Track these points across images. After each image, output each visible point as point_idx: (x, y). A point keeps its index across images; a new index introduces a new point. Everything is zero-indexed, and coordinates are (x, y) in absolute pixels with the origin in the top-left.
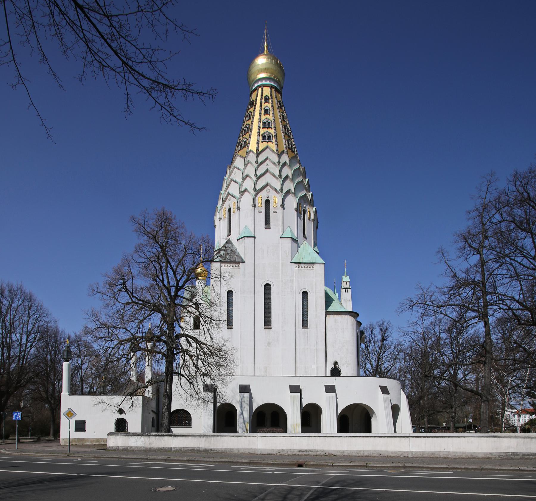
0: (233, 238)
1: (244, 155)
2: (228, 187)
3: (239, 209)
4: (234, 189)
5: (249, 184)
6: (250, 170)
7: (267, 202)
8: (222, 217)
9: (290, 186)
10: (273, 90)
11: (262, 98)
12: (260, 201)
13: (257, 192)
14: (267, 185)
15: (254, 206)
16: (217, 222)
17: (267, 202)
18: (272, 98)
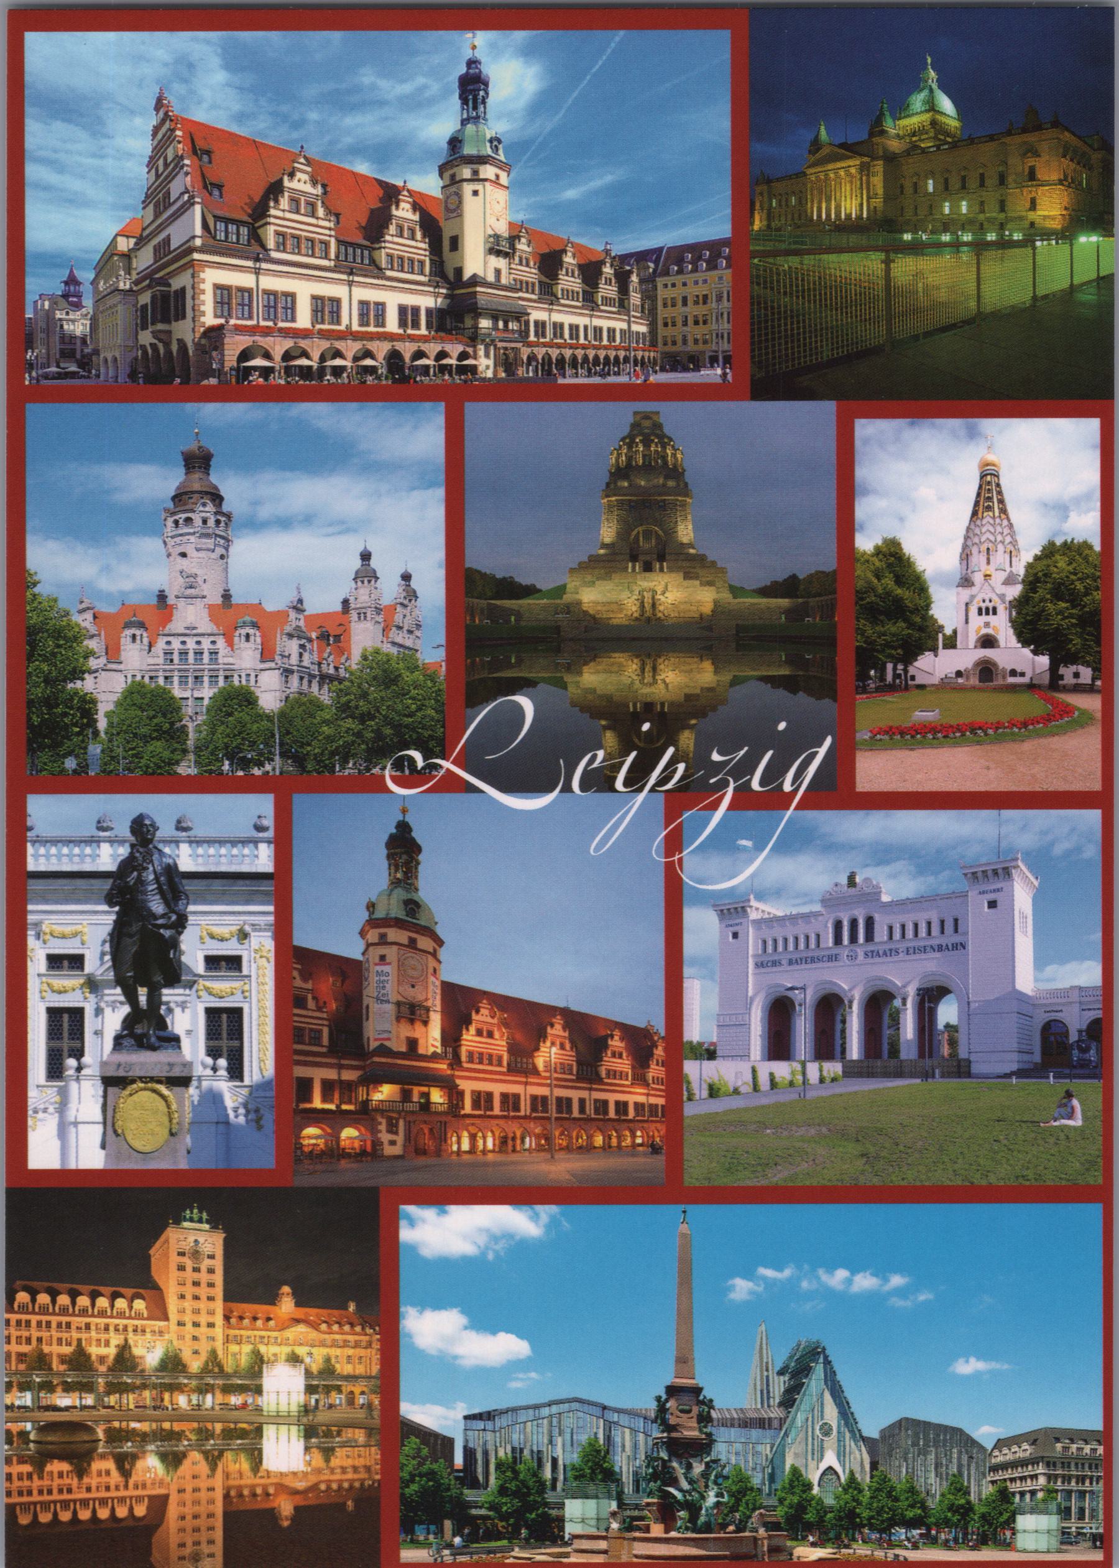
12: (984, 548)
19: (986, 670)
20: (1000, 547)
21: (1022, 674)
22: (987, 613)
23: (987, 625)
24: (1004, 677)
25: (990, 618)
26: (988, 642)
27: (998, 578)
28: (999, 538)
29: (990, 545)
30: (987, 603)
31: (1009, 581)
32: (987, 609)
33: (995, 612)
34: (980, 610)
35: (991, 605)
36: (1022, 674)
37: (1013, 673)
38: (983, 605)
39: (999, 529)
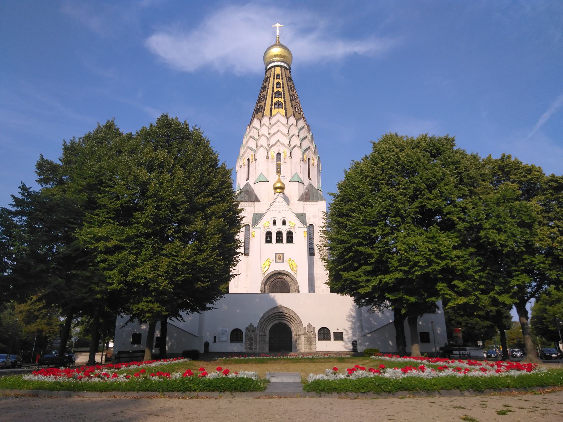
0: (251, 182)
1: (260, 118)
2: (247, 142)
3: (255, 159)
4: (252, 144)
5: (263, 141)
6: (264, 131)
7: (279, 154)
8: (242, 164)
9: (296, 141)
10: (283, 69)
11: (274, 76)
12: (273, 153)
13: (270, 147)
14: (278, 141)
15: (267, 157)
16: (238, 168)
17: (279, 154)
18: (282, 75)
21: (339, 336)
22: (279, 241)
23: (279, 257)
24: (310, 342)
25: (284, 247)
27: (294, 191)
30: (279, 226)
31: (308, 196)
32: (279, 234)
33: (290, 240)
37: (324, 334)
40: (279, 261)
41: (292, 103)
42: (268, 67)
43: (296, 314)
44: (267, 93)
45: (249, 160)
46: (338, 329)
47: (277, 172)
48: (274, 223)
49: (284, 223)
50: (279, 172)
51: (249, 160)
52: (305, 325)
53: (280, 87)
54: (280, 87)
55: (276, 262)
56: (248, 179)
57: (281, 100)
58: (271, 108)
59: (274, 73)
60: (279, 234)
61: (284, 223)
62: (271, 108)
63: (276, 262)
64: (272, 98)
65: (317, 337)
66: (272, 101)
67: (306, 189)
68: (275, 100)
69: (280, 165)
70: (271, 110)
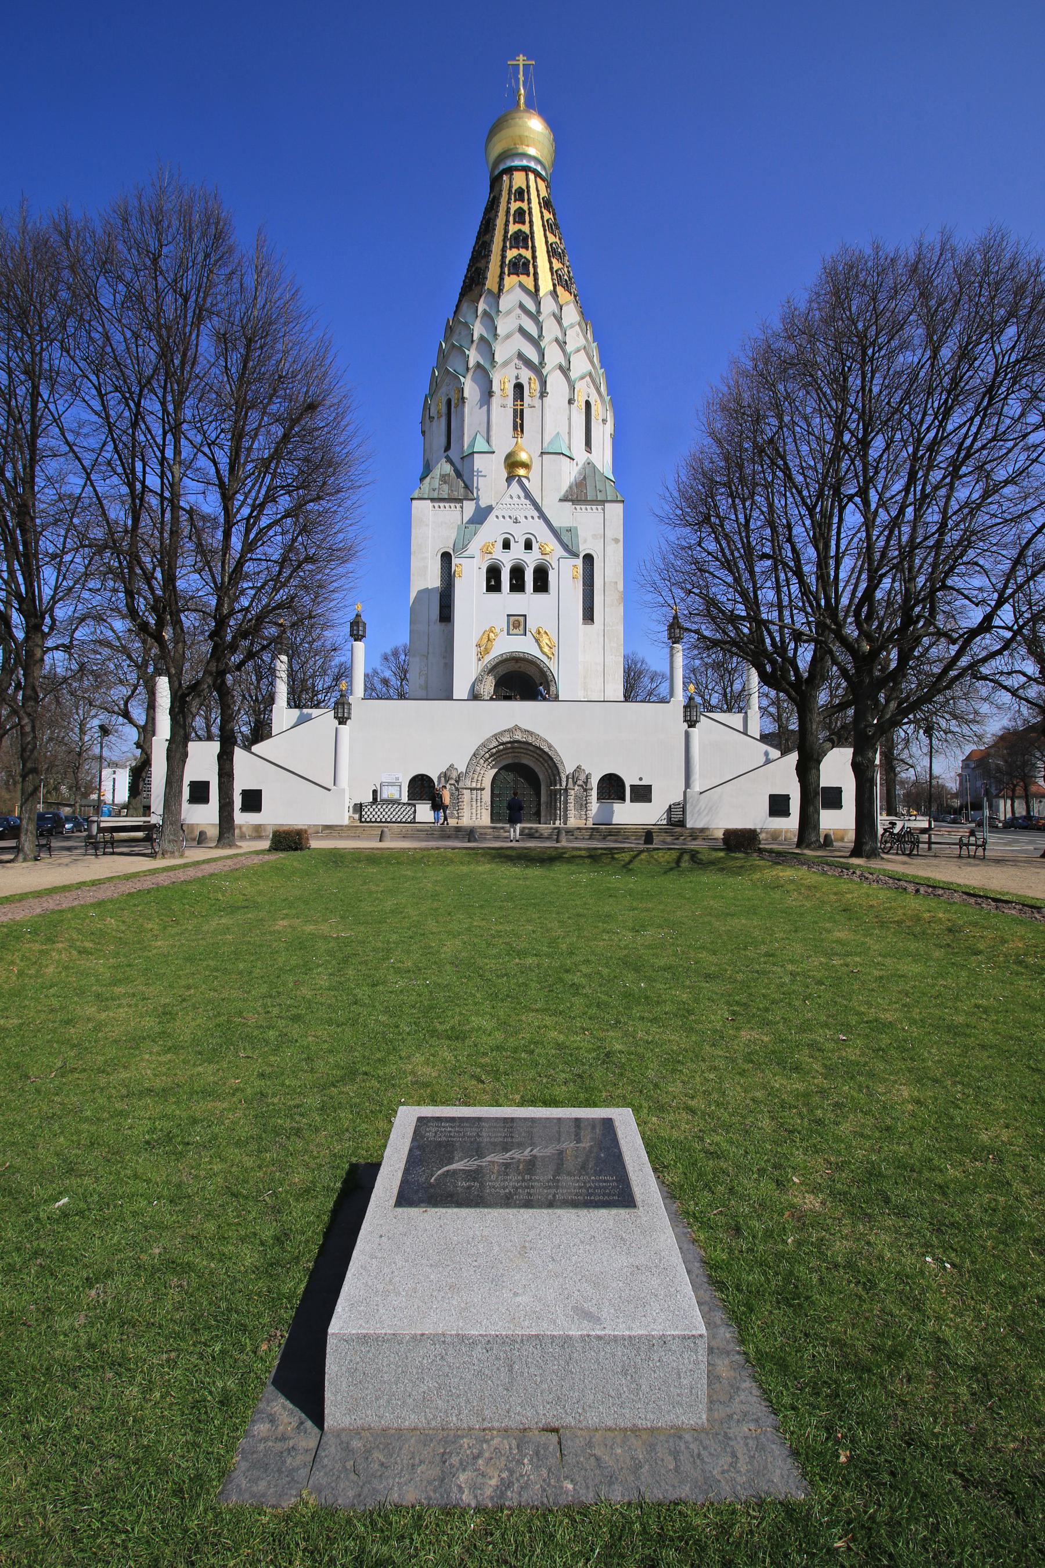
7: (519, 388)
10: (531, 176)
19: (525, 777)
20: (556, 382)
21: (642, 793)
22: (517, 586)
23: (517, 623)
25: (527, 602)
26: (521, 680)
28: (553, 357)
29: (526, 375)
32: (517, 573)
33: (542, 583)
34: (493, 574)
35: (531, 561)
36: (642, 793)
37: (612, 787)
38: (507, 561)
39: (551, 329)
40: (516, 631)
41: (551, 263)
42: (496, 173)
43: (550, 746)
44: (493, 237)
45: (449, 402)
46: (641, 779)
47: (515, 428)
48: (506, 545)
49: (528, 546)
50: (519, 427)
51: (449, 402)
52: (568, 767)
53: (524, 223)
54: (524, 223)
55: (508, 634)
56: (448, 448)
57: (528, 254)
58: (502, 273)
59: (511, 187)
60: (517, 573)
61: (528, 546)
62: (502, 273)
63: (508, 634)
64: (504, 250)
65: (594, 793)
66: (503, 257)
67: (580, 474)
68: (511, 254)
69: (522, 411)
70: (501, 278)
